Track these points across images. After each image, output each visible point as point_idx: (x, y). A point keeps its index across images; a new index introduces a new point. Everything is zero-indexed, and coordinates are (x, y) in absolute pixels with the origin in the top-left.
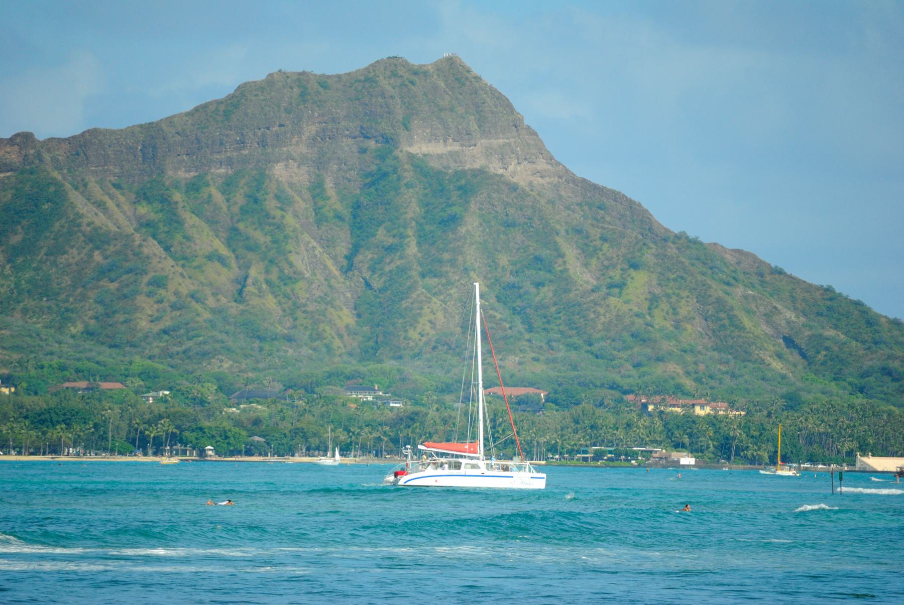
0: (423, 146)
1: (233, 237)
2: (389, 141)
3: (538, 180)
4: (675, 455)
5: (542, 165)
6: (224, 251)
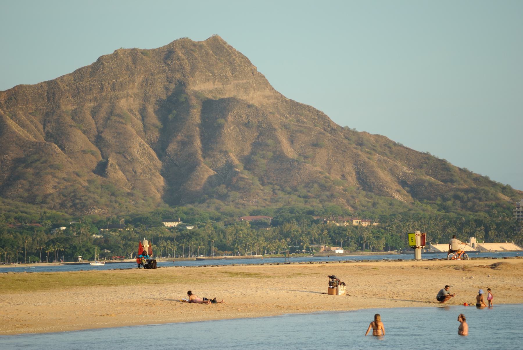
0: (201, 86)
1: (99, 141)
2: (182, 85)
3: (265, 102)
4: (332, 248)
5: (267, 92)
6: (94, 148)
